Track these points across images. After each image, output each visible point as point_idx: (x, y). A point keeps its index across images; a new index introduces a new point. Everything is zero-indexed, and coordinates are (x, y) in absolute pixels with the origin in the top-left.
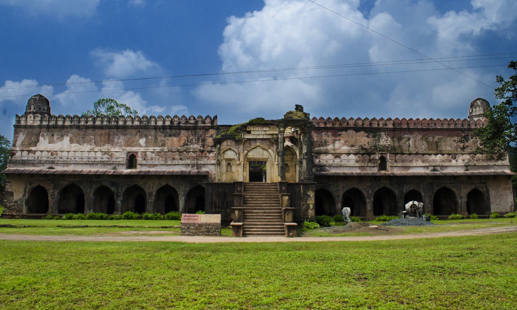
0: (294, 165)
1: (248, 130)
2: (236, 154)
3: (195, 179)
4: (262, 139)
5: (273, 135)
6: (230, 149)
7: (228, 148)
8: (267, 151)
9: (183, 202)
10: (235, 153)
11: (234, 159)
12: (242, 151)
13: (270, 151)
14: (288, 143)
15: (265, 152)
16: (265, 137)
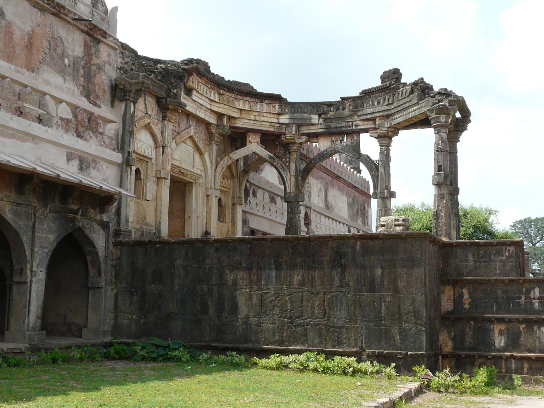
0: (231, 205)
1: (190, 84)
2: (157, 146)
3: (75, 207)
4: (200, 120)
5: (220, 116)
6: (148, 127)
7: (147, 121)
8: (201, 154)
9: (42, 288)
10: (151, 142)
11: (151, 159)
12: (170, 139)
13: (206, 156)
14: (254, 146)
15: (197, 156)
16: (207, 118)
